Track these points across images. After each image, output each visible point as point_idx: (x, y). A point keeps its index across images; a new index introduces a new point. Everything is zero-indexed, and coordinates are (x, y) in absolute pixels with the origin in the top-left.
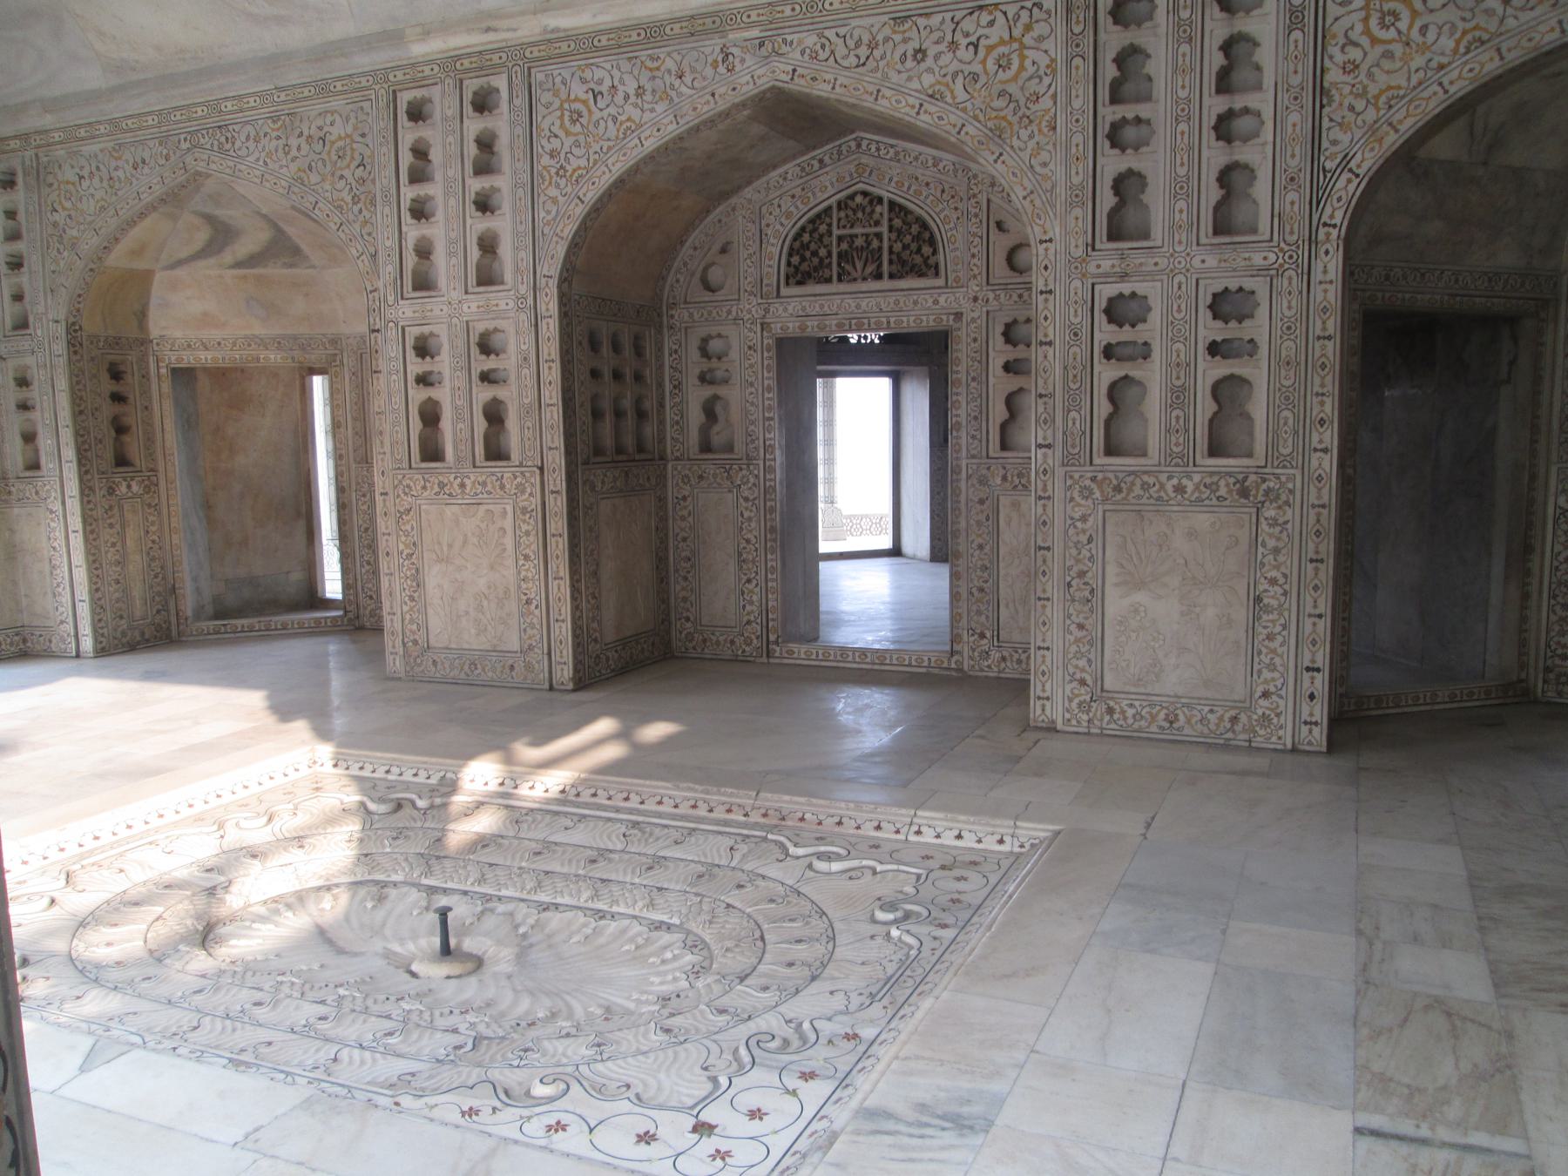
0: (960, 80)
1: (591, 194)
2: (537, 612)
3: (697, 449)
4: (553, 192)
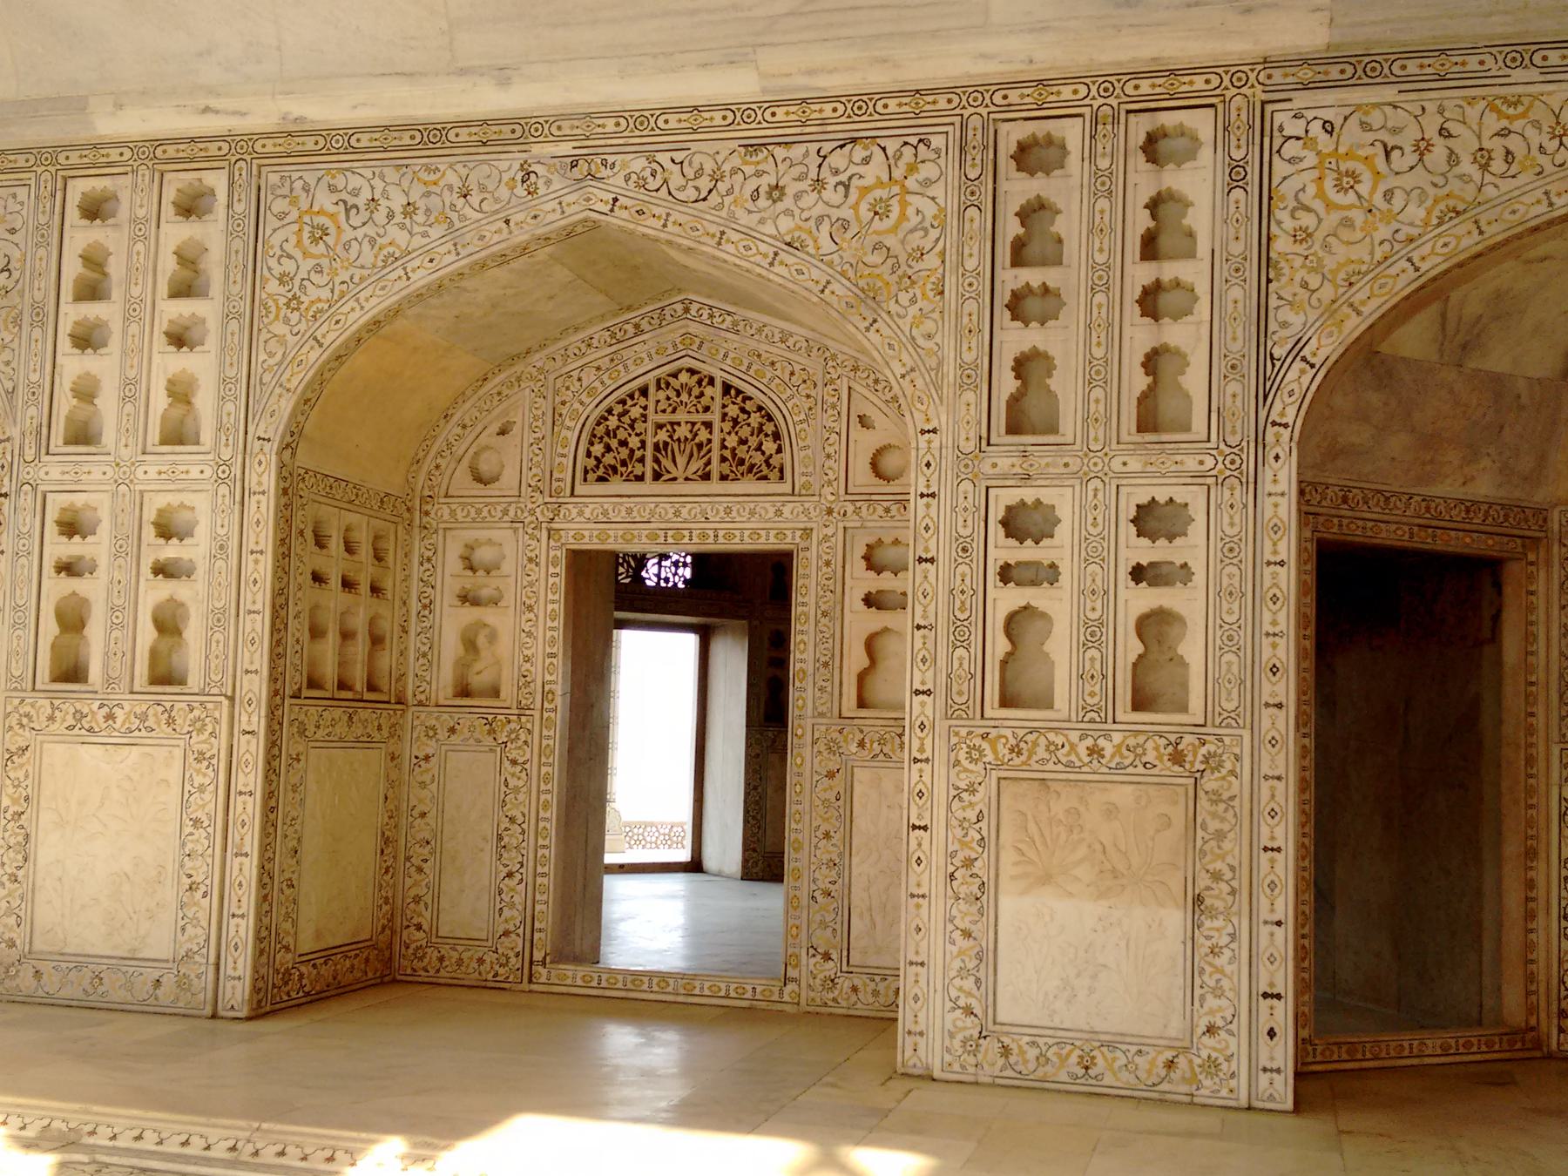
0: (825, 227)
1: (333, 337)
3: (450, 691)
4: (280, 328)
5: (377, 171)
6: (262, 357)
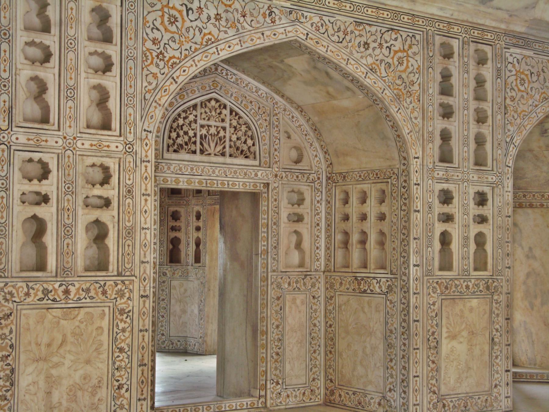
0: (383, 64)
2: (127, 395)
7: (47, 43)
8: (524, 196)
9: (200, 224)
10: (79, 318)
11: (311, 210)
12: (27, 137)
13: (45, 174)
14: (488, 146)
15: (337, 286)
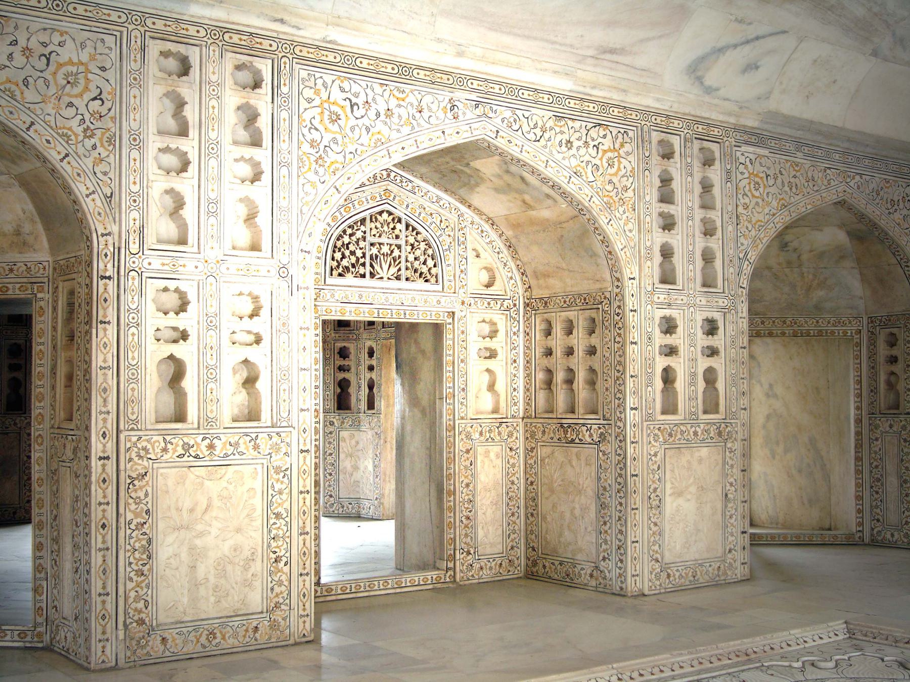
0: (590, 166)
1: (348, 187)
4: (311, 176)
5: (369, 84)
6: (302, 194)
7: (184, 148)
8: (763, 323)
9: (374, 362)
10: (226, 478)
11: (506, 343)
12: (161, 261)
13: (183, 307)
14: (718, 264)
15: (539, 435)
